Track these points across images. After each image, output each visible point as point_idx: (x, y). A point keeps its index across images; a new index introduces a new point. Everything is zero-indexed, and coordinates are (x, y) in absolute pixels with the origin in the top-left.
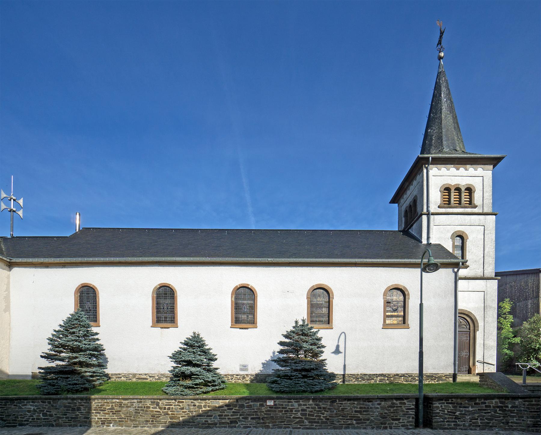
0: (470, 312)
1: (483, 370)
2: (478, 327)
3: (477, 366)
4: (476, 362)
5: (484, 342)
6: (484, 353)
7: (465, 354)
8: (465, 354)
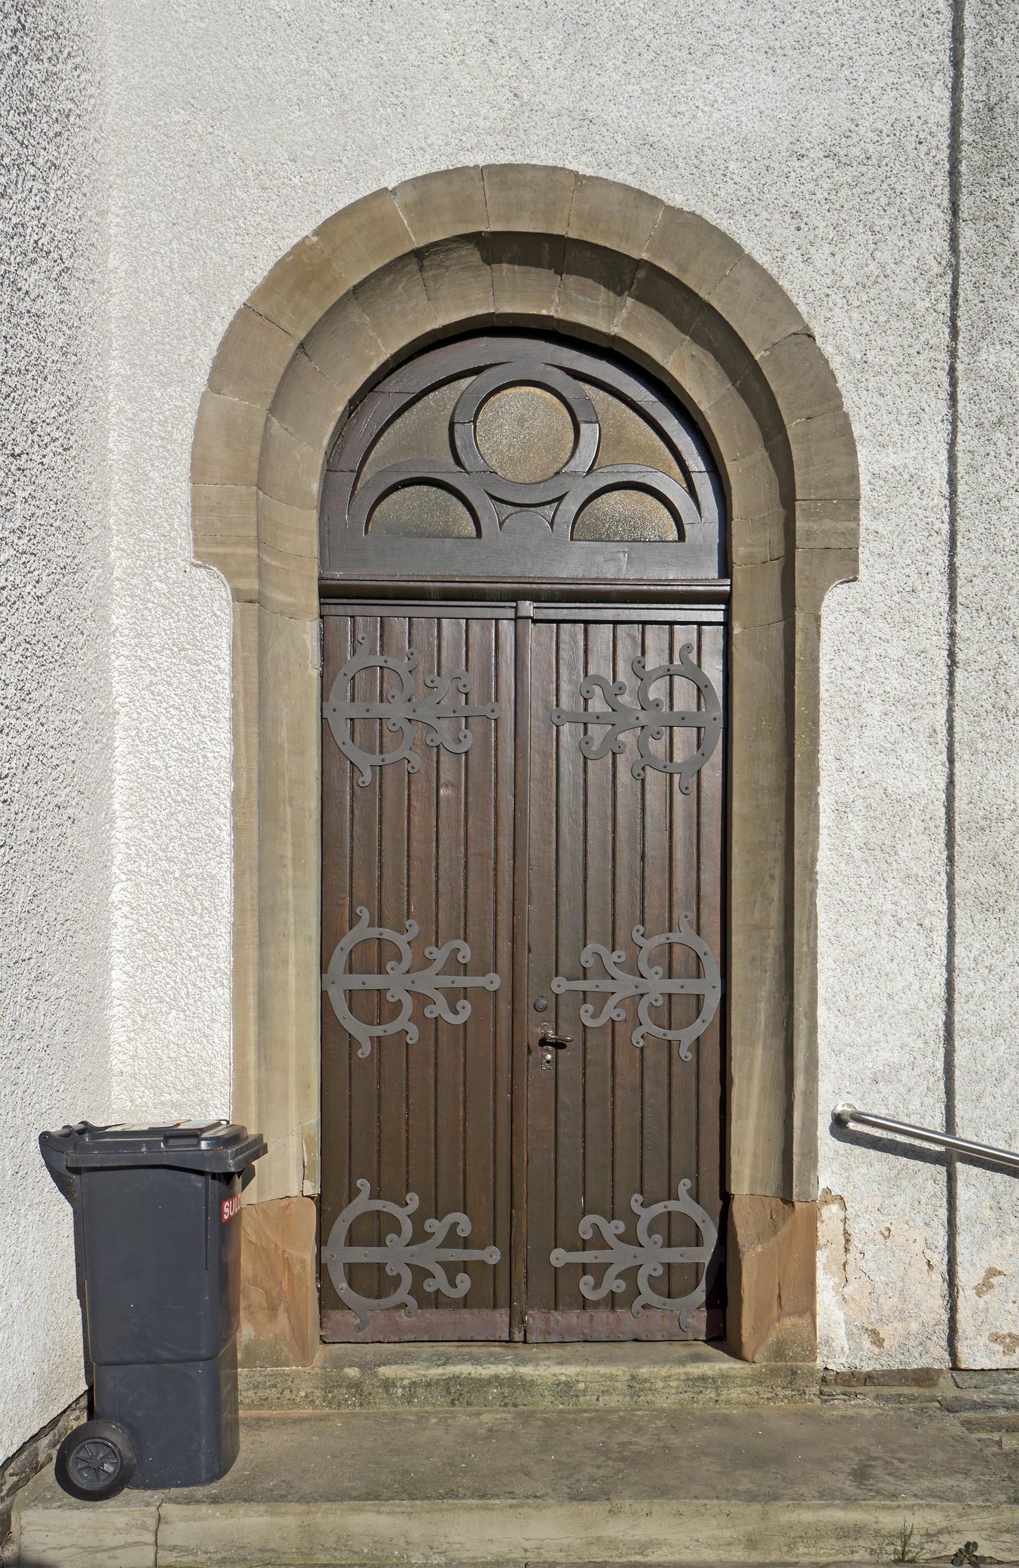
0: (696, 222)
1: (940, 1287)
2: (854, 502)
3: (830, 1213)
4: (827, 1143)
5: (951, 782)
6: (959, 985)
7: (657, 985)
8: (657, 985)
